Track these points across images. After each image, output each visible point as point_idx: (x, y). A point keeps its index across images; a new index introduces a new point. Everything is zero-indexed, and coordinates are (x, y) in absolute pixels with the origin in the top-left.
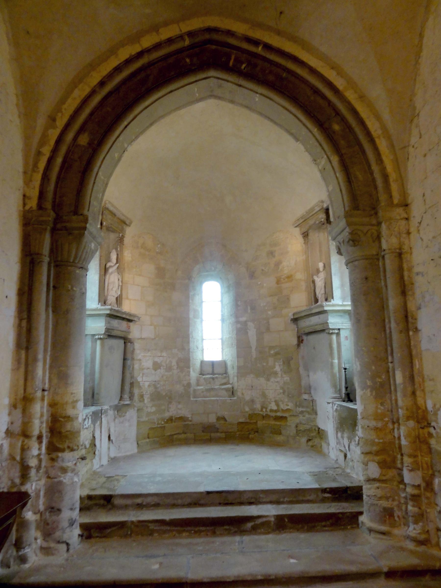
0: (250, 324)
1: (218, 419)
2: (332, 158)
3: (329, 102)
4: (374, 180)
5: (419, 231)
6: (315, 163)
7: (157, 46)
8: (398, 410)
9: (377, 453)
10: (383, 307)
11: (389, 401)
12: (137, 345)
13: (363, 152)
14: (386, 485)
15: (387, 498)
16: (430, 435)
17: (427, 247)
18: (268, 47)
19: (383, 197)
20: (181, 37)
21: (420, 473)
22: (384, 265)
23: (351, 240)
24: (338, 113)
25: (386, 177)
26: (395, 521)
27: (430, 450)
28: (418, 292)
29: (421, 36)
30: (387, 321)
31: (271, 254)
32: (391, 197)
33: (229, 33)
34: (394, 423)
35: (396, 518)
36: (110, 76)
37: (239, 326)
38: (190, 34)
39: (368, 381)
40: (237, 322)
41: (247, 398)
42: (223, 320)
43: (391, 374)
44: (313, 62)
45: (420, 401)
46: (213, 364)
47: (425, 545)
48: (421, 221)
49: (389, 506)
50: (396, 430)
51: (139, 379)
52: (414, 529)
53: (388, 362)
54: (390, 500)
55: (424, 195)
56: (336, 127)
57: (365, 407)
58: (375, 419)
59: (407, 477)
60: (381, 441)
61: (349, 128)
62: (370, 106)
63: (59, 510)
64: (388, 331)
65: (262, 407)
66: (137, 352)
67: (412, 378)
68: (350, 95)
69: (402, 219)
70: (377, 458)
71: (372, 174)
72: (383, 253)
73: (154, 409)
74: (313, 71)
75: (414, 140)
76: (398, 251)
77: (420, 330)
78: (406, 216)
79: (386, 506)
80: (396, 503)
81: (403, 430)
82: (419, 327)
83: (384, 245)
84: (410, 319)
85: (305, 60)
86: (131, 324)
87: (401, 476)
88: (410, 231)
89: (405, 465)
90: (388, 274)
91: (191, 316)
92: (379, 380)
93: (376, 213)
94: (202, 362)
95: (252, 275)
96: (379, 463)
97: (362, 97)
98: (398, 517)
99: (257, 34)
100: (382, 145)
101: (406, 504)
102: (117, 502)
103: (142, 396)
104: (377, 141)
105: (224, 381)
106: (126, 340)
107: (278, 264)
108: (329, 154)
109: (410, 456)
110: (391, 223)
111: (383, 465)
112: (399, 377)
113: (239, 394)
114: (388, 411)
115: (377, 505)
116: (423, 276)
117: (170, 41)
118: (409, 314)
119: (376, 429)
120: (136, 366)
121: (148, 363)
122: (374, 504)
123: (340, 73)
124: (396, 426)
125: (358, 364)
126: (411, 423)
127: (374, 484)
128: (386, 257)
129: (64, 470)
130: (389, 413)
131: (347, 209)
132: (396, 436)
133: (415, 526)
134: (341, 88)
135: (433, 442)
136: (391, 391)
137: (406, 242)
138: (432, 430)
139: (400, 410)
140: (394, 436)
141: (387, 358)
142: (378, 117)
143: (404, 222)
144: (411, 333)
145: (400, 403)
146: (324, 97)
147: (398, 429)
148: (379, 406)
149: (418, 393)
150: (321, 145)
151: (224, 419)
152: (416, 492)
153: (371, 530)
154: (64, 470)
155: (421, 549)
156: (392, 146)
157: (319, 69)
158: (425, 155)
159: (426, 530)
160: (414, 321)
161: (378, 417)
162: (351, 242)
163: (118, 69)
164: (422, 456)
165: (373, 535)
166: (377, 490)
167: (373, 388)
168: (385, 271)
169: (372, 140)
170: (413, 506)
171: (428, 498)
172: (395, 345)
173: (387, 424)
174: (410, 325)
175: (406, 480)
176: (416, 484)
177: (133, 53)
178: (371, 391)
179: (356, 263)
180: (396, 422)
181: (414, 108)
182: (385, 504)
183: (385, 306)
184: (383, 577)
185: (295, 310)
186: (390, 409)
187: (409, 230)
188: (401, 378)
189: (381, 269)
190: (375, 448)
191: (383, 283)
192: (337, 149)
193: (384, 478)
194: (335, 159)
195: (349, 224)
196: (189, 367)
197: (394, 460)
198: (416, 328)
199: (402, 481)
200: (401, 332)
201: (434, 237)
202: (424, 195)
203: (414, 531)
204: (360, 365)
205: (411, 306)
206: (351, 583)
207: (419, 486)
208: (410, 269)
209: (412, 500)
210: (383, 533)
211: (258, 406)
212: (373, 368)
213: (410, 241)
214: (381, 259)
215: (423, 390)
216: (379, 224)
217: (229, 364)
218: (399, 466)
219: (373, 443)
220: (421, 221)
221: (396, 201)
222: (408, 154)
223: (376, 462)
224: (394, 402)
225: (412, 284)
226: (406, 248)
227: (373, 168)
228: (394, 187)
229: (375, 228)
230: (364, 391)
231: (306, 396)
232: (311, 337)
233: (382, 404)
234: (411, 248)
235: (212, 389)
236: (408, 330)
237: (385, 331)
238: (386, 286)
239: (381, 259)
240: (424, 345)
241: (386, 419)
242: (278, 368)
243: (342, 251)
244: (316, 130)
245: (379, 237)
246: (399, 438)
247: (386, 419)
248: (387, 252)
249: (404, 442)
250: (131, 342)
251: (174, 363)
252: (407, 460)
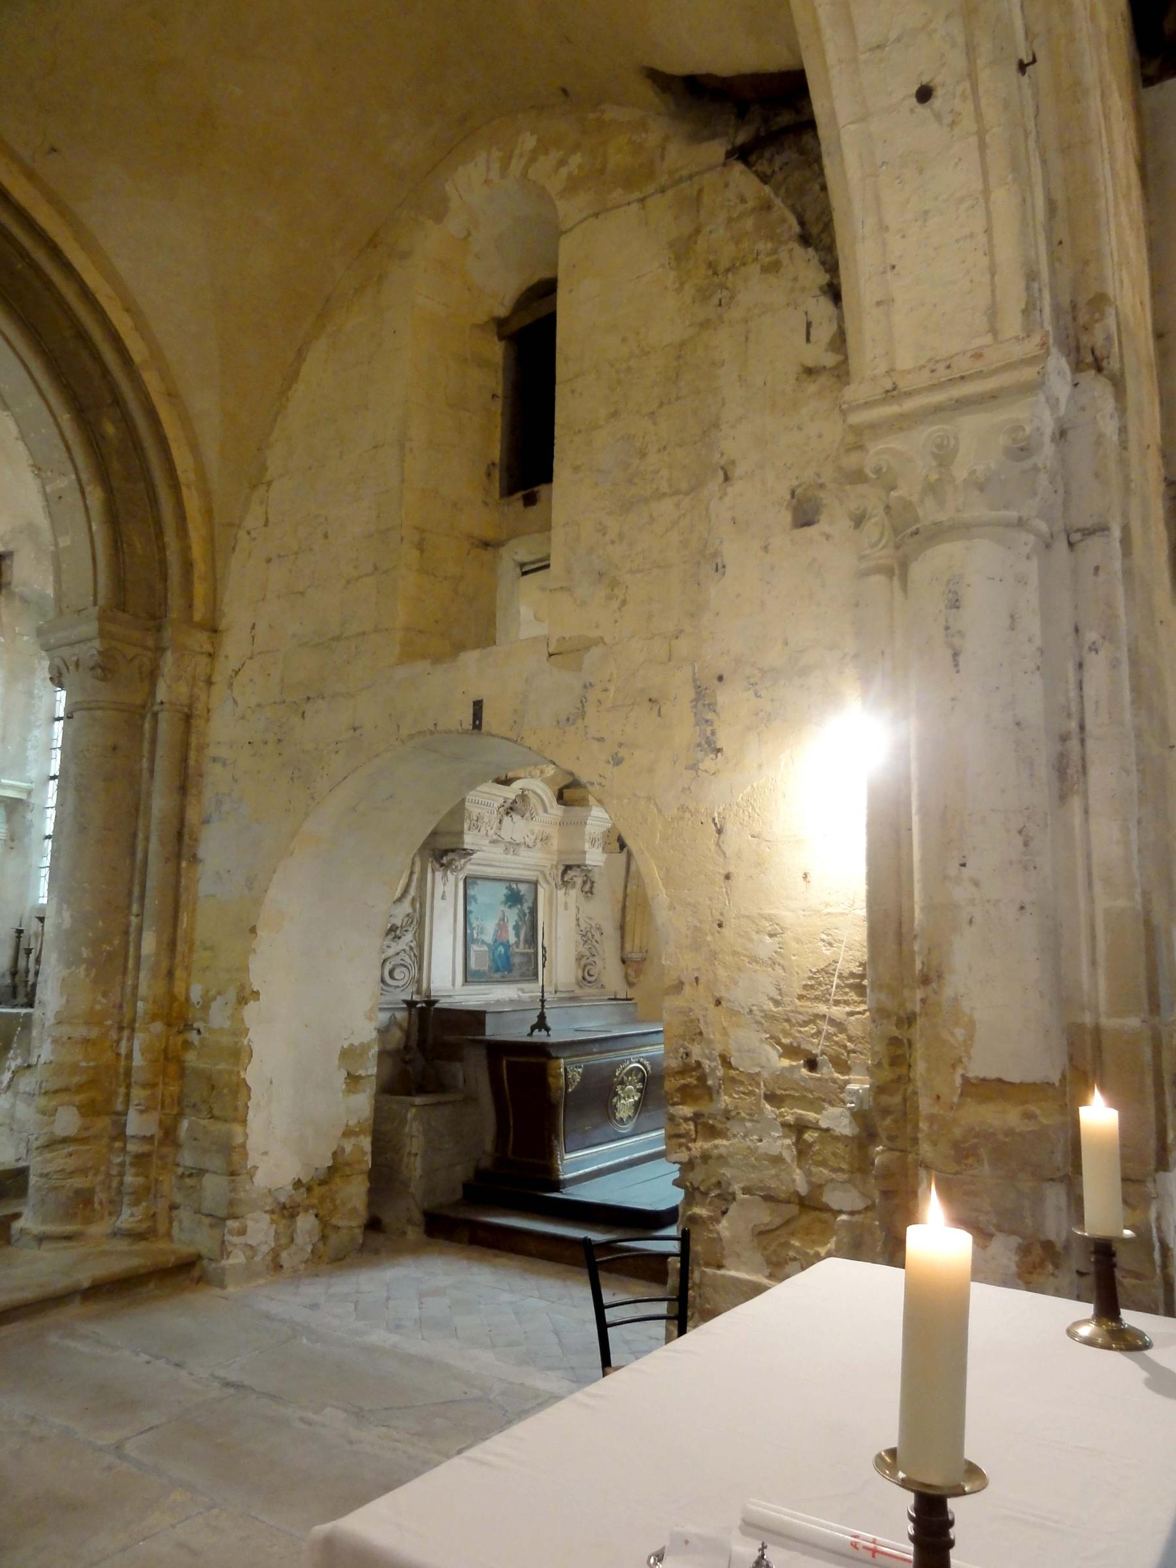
2: (88, 489)
3: (106, 372)
4: (163, 562)
5: (231, 684)
6: (36, 472)
8: (135, 1005)
9: (80, 1088)
10: (137, 810)
11: (118, 988)
13: (154, 501)
14: (88, 1147)
15: (83, 1171)
16: (187, 1045)
17: (243, 718)
19: (175, 601)
21: (154, 1117)
22: (155, 729)
23: (100, 667)
24: (118, 401)
25: (188, 566)
26: (94, 1210)
27: (182, 1073)
28: (208, 794)
29: (300, 355)
30: (141, 835)
32: (191, 606)
34: (121, 1028)
35: (97, 1206)
39: (83, 949)
43: (132, 938)
44: (92, 278)
45: (179, 987)
47: (146, 1239)
48: (239, 670)
49: (87, 1185)
50: (124, 1043)
52: (132, 1215)
53: (129, 913)
54: (90, 1174)
55: (253, 627)
56: (110, 429)
57: (68, 1001)
58: (87, 1023)
59: (135, 1124)
60: (92, 1064)
61: (137, 446)
62: (185, 419)
64: (140, 855)
67: (172, 944)
68: (151, 380)
69: (202, 653)
70: (78, 1099)
71: (162, 548)
72: (156, 708)
75: (252, 521)
76: (186, 710)
77: (201, 861)
78: (211, 650)
79: (80, 1186)
80: (100, 1178)
82: (202, 853)
83: (162, 694)
84: (186, 837)
88: (214, 679)
89: (134, 1101)
90: (160, 752)
92: (108, 948)
93: (159, 629)
96: (80, 1107)
97: (172, 395)
98: (101, 1203)
100: (192, 503)
101: (121, 1174)
104: (185, 491)
108: (84, 477)
109: (145, 1086)
110: (183, 655)
111: (89, 1110)
112: (149, 944)
114: (114, 1006)
115: (63, 1187)
116: (224, 765)
118: (186, 830)
119: (86, 1041)
122: (56, 1188)
123: (142, 328)
124: (126, 1033)
125: (66, 915)
126: (158, 1027)
127: (63, 1149)
128: (163, 717)
130: (115, 1011)
131: (101, 601)
132: (123, 1051)
133: (134, 1209)
134: (137, 359)
135: (191, 1058)
136: (125, 968)
137: (203, 697)
138: (193, 1036)
139: (140, 1004)
140: (118, 1055)
141: (129, 907)
142: (194, 447)
143: (205, 660)
144: (184, 864)
145: (143, 990)
146: (97, 357)
147: (131, 1039)
148: (100, 998)
149: (179, 973)
150: (68, 449)
152: (145, 1148)
153: (41, 1239)
155: (141, 1246)
156: (208, 512)
158: (269, 561)
159: (152, 1213)
160: (191, 843)
161: (93, 1018)
162: (99, 671)
164: (165, 1084)
165: (46, 1246)
166: (68, 1160)
167: (91, 964)
168: (153, 741)
169: (175, 486)
170: (136, 1175)
171: (162, 1157)
172: (151, 884)
173: (109, 1031)
174: (185, 850)
175: (130, 1130)
176: (148, 1134)
178: (87, 970)
179: (98, 713)
180: (127, 1026)
181: (263, 468)
182: (79, 1182)
183: (142, 808)
184: (78, 1299)
186: (118, 1001)
187: (210, 677)
188: (154, 944)
189: (147, 735)
190: (76, 1079)
191: (145, 764)
192: (104, 477)
193: (86, 1134)
194: (96, 496)
195: (102, 634)
197: (111, 1095)
198: (194, 856)
199: (120, 1134)
200: (167, 860)
201: (259, 705)
202: (253, 627)
203: (132, 1219)
204: (72, 916)
205: (192, 815)
206: (18, 1324)
207: (152, 1138)
208: (201, 748)
209: (132, 1164)
210: (68, 1238)
212: (101, 923)
213: (209, 697)
214: (149, 716)
215: (187, 968)
216: (160, 650)
218: (119, 1107)
219: (75, 1069)
220: (239, 670)
221: (197, 617)
222: (236, 541)
223: (74, 1105)
224: (128, 990)
225: (201, 776)
226: (200, 707)
227: (166, 539)
228: (200, 590)
229: (150, 654)
230: (74, 968)
233: (105, 994)
234: (209, 711)
236: (178, 856)
237: (133, 852)
238: (152, 771)
239: (149, 716)
240: (205, 887)
241: (109, 1022)
243: (66, 680)
244: (67, 416)
245: (152, 676)
246: (129, 1056)
247: (109, 1022)
248: (166, 706)
249: (138, 1060)
252: (138, 1094)
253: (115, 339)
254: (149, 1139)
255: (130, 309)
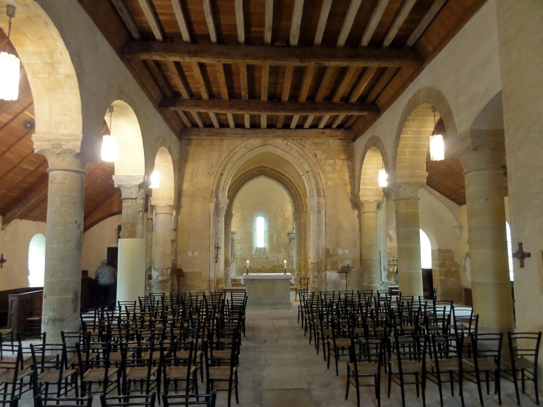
0: (274, 234)
1: (262, 267)
7: (249, 171)
12: (235, 242)
18: (276, 171)
20: (254, 168)
25: (303, 205)
31: (282, 210)
33: (267, 167)
36: (237, 179)
37: (270, 235)
38: (257, 168)
40: (270, 234)
41: (272, 260)
42: (264, 232)
44: (287, 175)
46: (260, 248)
51: (236, 253)
56: (292, 191)
59: (303, 273)
63: (228, 279)
65: (277, 263)
66: (236, 244)
73: (241, 263)
74: (287, 177)
81: (303, 263)
85: (285, 174)
86: (234, 235)
87: (302, 273)
91: (253, 231)
94: (256, 247)
95: (275, 217)
97: (298, 185)
99: (273, 168)
102: (237, 281)
103: (237, 258)
105: (264, 254)
106: (232, 240)
107: (284, 214)
113: (270, 259)
117: (252, 169)
120: (235, 249)
121: (239, 248)
129: (228, 271)
134: (293, 182)
151: (264, 267)
154: (228, 271)
157: (289, 178)
163: (239, 177)
177: (243, 173)
180: (302, 262)
185: (289, 231)
194: (292, 199)
195: (294, 216)
196: (252, 249)
211: (276, 263)
217: (266, 248)
228: (304, 207)
231: (291, 259)
232: (293, 240)
235: (261, 257)
242: (283, 250)
245: (300, 219)
249: (303, 266)
250: (234, 240)
251: (247, 247)
252: (303, 269)
253: (290, 181)
254: (304, 275)
255: (292, 177)
